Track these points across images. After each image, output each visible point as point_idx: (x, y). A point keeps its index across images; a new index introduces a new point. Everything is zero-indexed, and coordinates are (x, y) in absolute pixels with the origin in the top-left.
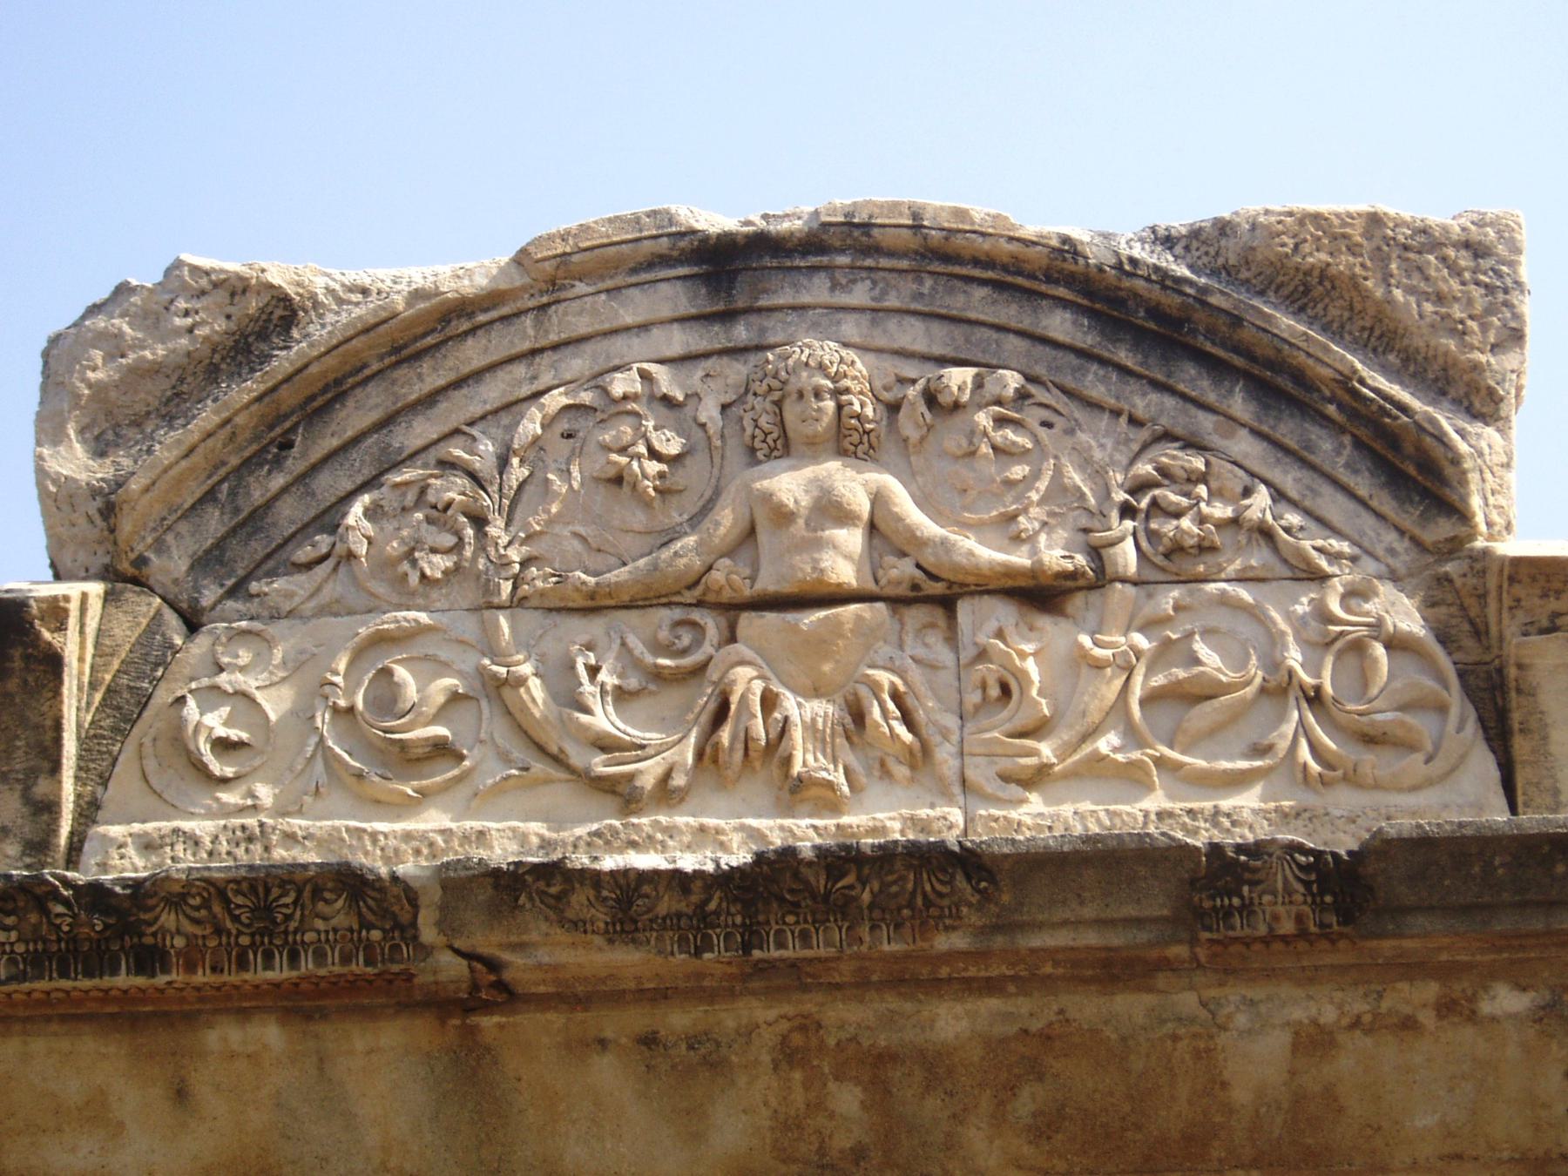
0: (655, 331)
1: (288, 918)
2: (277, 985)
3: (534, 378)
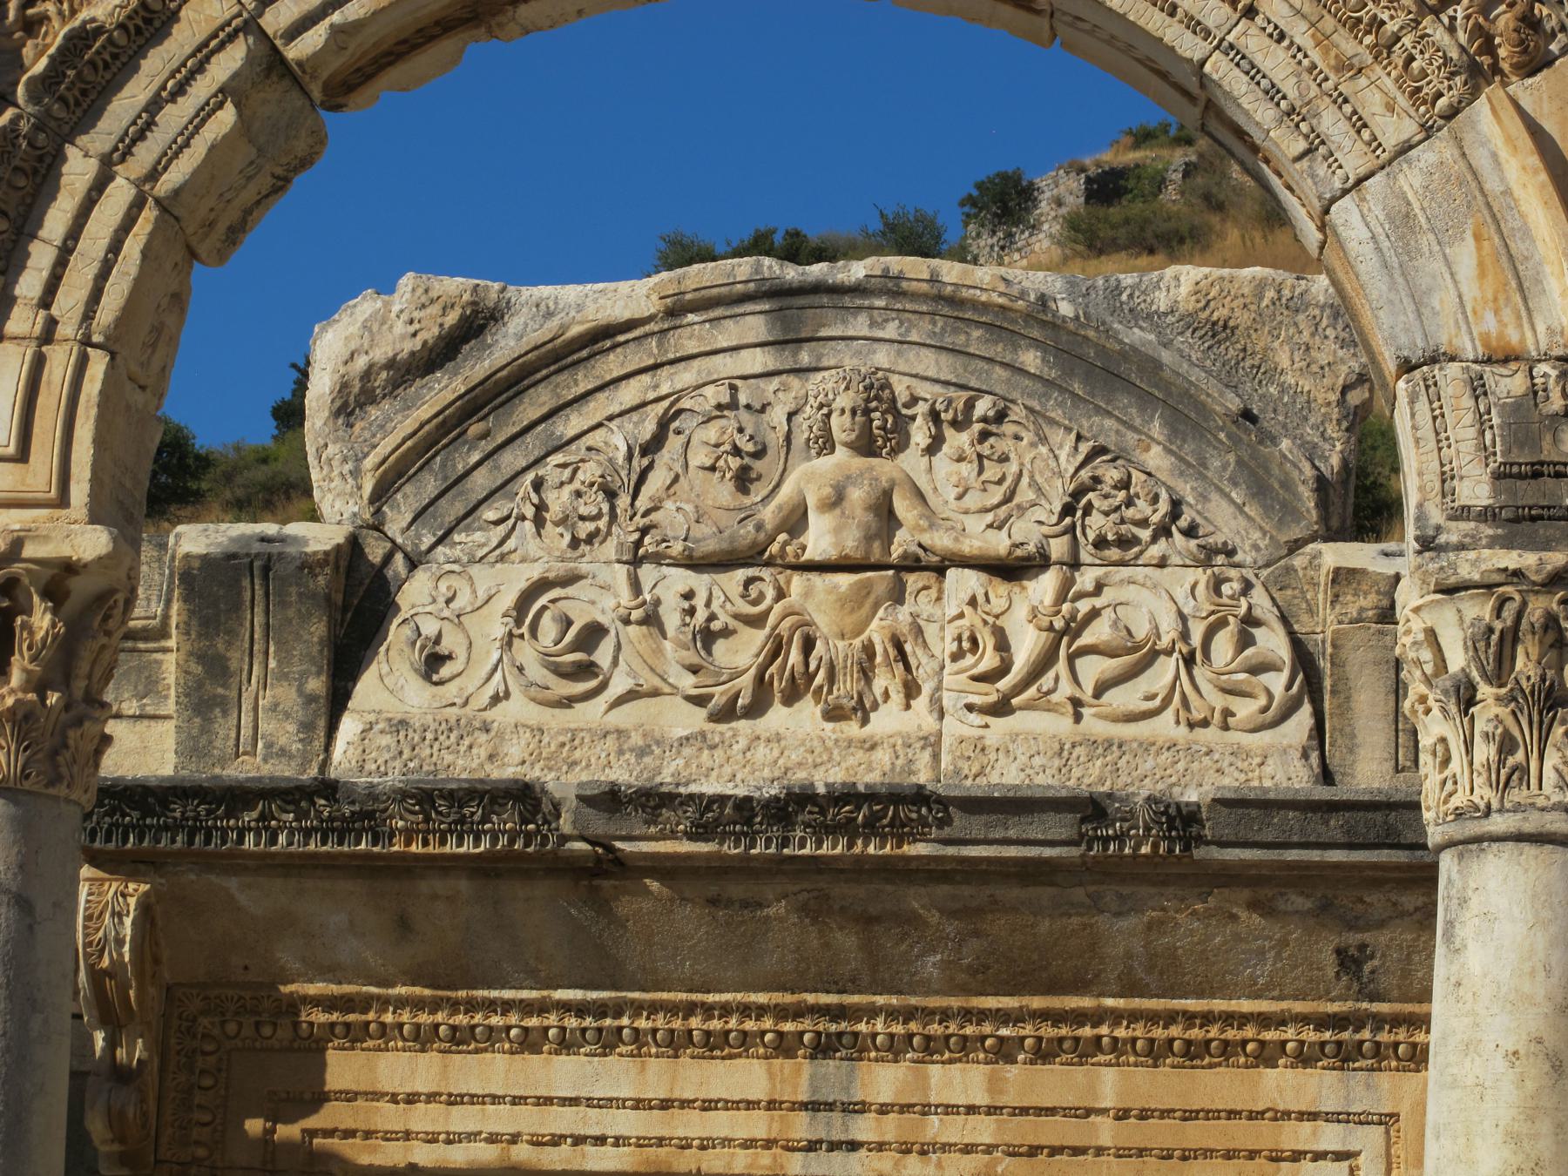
0: (744, 353)
1: (473, 814)
3: (656, 387)
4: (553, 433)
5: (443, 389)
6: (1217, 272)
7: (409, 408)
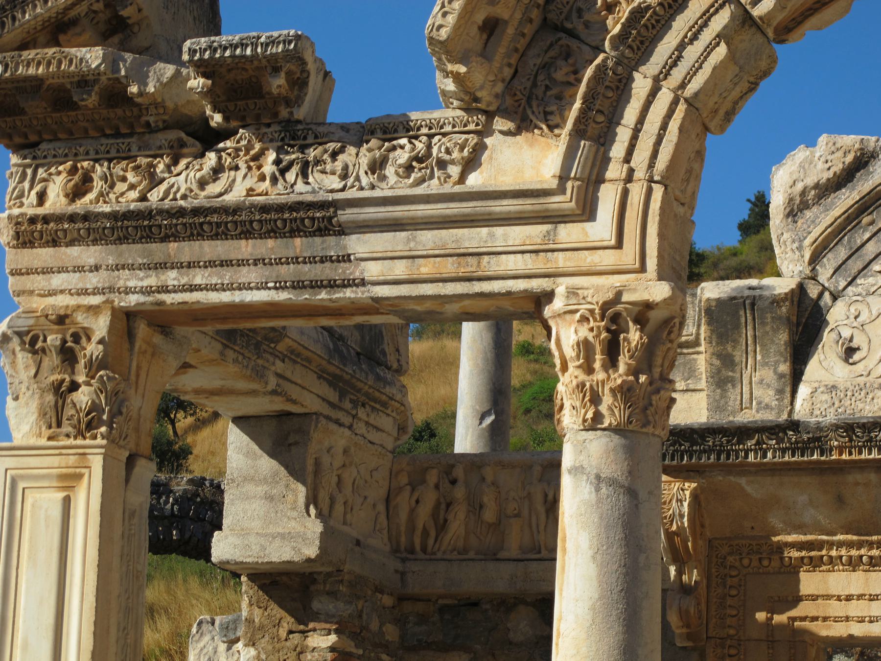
1: (876, 436)
5: (846, 199)
7: (828, 210)
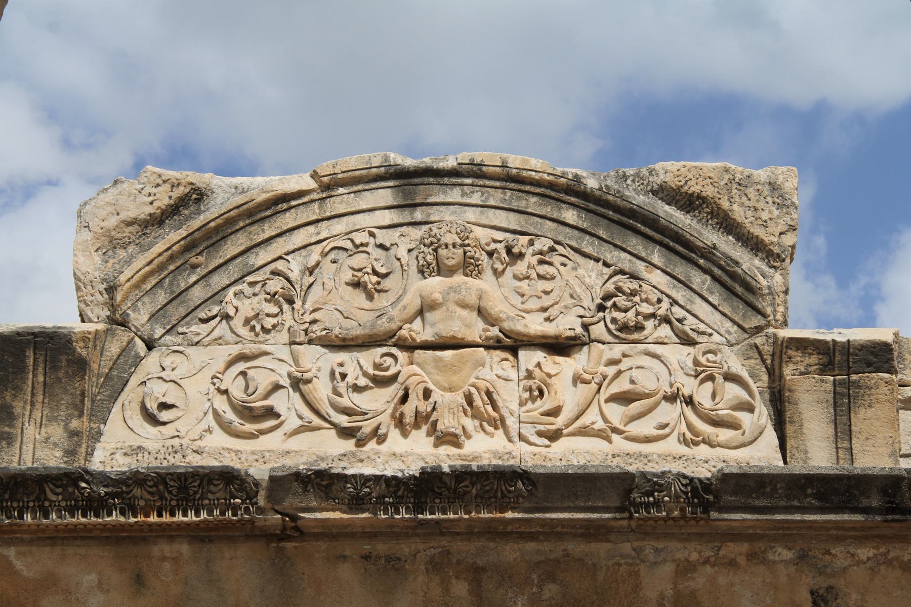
0: (377, 212)
1: (196, 493)
2: (188, 525)
3: (318, 233)
4: (247, 263)
6: (690, 164)
